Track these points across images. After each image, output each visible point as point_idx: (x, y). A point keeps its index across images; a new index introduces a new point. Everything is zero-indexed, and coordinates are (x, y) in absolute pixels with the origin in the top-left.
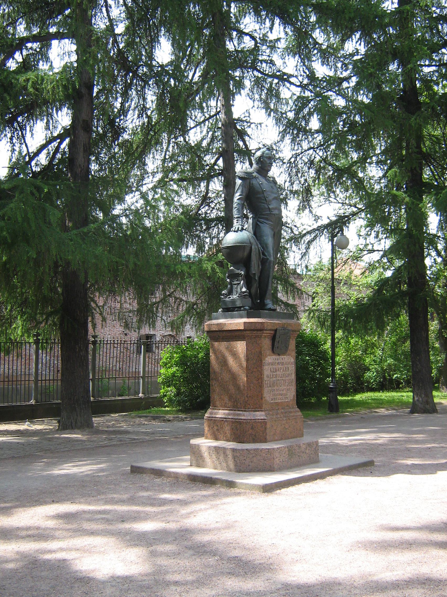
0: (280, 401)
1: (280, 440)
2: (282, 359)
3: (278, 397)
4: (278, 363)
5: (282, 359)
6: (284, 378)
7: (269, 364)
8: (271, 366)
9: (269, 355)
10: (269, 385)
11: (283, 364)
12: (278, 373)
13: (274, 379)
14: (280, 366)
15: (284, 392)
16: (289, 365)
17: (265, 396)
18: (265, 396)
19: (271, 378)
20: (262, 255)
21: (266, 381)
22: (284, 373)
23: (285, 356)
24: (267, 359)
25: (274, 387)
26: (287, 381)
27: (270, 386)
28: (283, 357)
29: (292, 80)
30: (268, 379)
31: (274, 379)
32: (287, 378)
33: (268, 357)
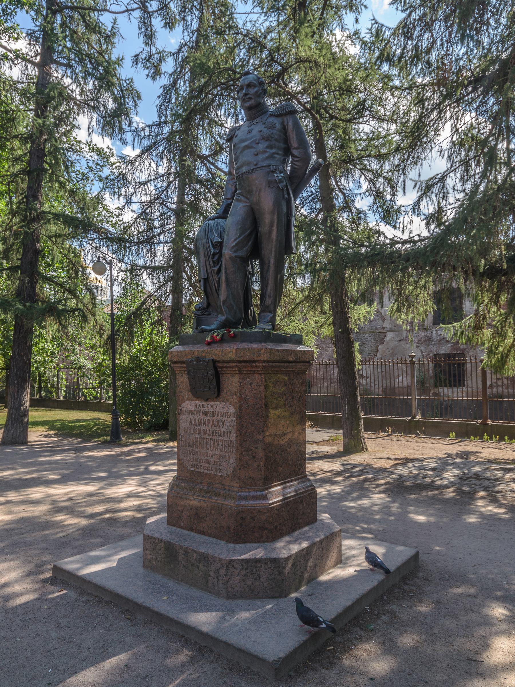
0: (206, 471)
2: (212, 407)
3: (203, 464)
4: (204, 413)
5: (212, 407)
6: (215, 438)
7: (188, 412)
8: (191, 416)
9: (188, 399)
11: (213, 414)
12: (203, 427)
13: (197, 436)
14: (208, 418)
16: (226, 418)
20: (212, 248)
23: (217, 403)
24: (184, 404)
25: (196, 447)
26: (221, 443)
27: (189, 446)
28: (212, 403)
32: (220, 438)
33: (187, 402)
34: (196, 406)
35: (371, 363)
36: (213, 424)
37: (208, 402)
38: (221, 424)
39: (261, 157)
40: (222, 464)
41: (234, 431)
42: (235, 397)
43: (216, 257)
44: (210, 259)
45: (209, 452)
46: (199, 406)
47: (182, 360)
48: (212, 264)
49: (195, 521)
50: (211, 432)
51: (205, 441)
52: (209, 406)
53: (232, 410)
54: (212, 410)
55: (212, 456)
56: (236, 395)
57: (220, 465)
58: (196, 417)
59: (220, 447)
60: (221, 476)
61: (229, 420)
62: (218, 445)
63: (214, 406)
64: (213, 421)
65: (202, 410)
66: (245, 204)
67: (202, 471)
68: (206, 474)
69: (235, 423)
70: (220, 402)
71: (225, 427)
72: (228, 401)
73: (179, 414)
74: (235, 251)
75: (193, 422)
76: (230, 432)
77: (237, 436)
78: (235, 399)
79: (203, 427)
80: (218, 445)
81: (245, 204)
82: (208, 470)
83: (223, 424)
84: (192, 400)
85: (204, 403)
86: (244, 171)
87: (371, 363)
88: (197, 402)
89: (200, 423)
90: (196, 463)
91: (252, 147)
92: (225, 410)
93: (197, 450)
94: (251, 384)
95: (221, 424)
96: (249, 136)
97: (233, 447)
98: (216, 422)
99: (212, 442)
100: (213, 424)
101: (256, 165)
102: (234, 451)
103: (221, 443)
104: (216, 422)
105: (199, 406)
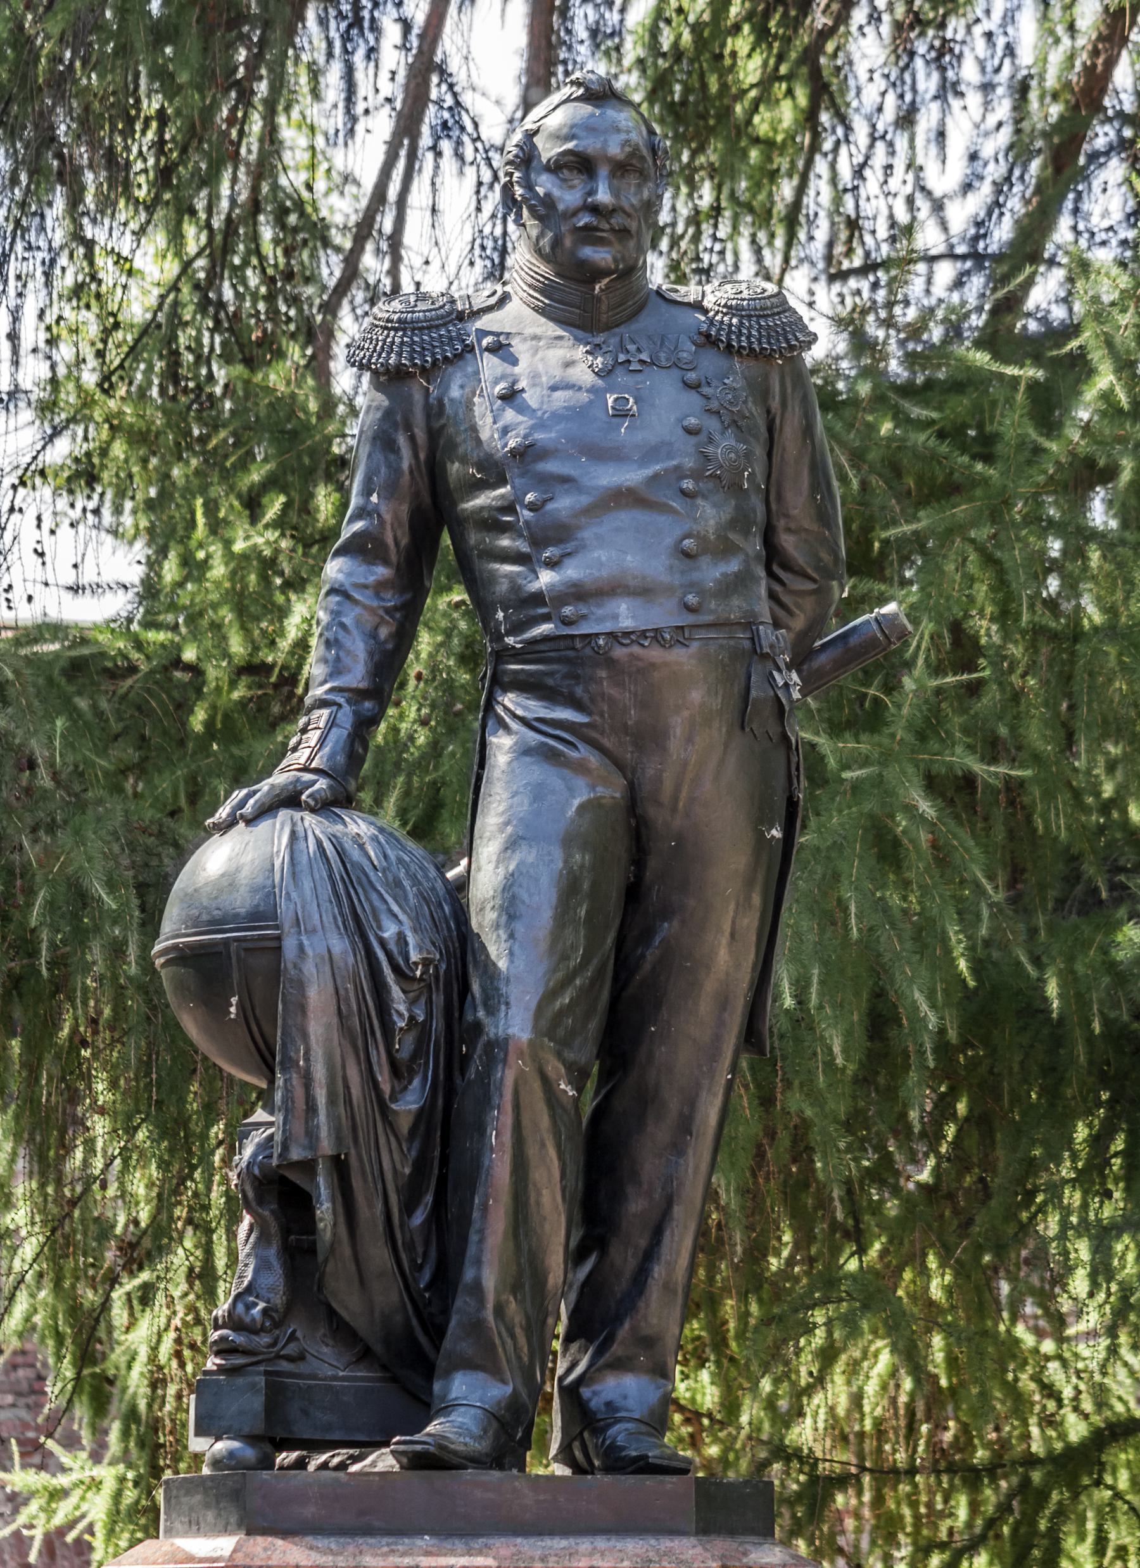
20: (396, 992)
39: (713, 572)
48: (384, 1079)
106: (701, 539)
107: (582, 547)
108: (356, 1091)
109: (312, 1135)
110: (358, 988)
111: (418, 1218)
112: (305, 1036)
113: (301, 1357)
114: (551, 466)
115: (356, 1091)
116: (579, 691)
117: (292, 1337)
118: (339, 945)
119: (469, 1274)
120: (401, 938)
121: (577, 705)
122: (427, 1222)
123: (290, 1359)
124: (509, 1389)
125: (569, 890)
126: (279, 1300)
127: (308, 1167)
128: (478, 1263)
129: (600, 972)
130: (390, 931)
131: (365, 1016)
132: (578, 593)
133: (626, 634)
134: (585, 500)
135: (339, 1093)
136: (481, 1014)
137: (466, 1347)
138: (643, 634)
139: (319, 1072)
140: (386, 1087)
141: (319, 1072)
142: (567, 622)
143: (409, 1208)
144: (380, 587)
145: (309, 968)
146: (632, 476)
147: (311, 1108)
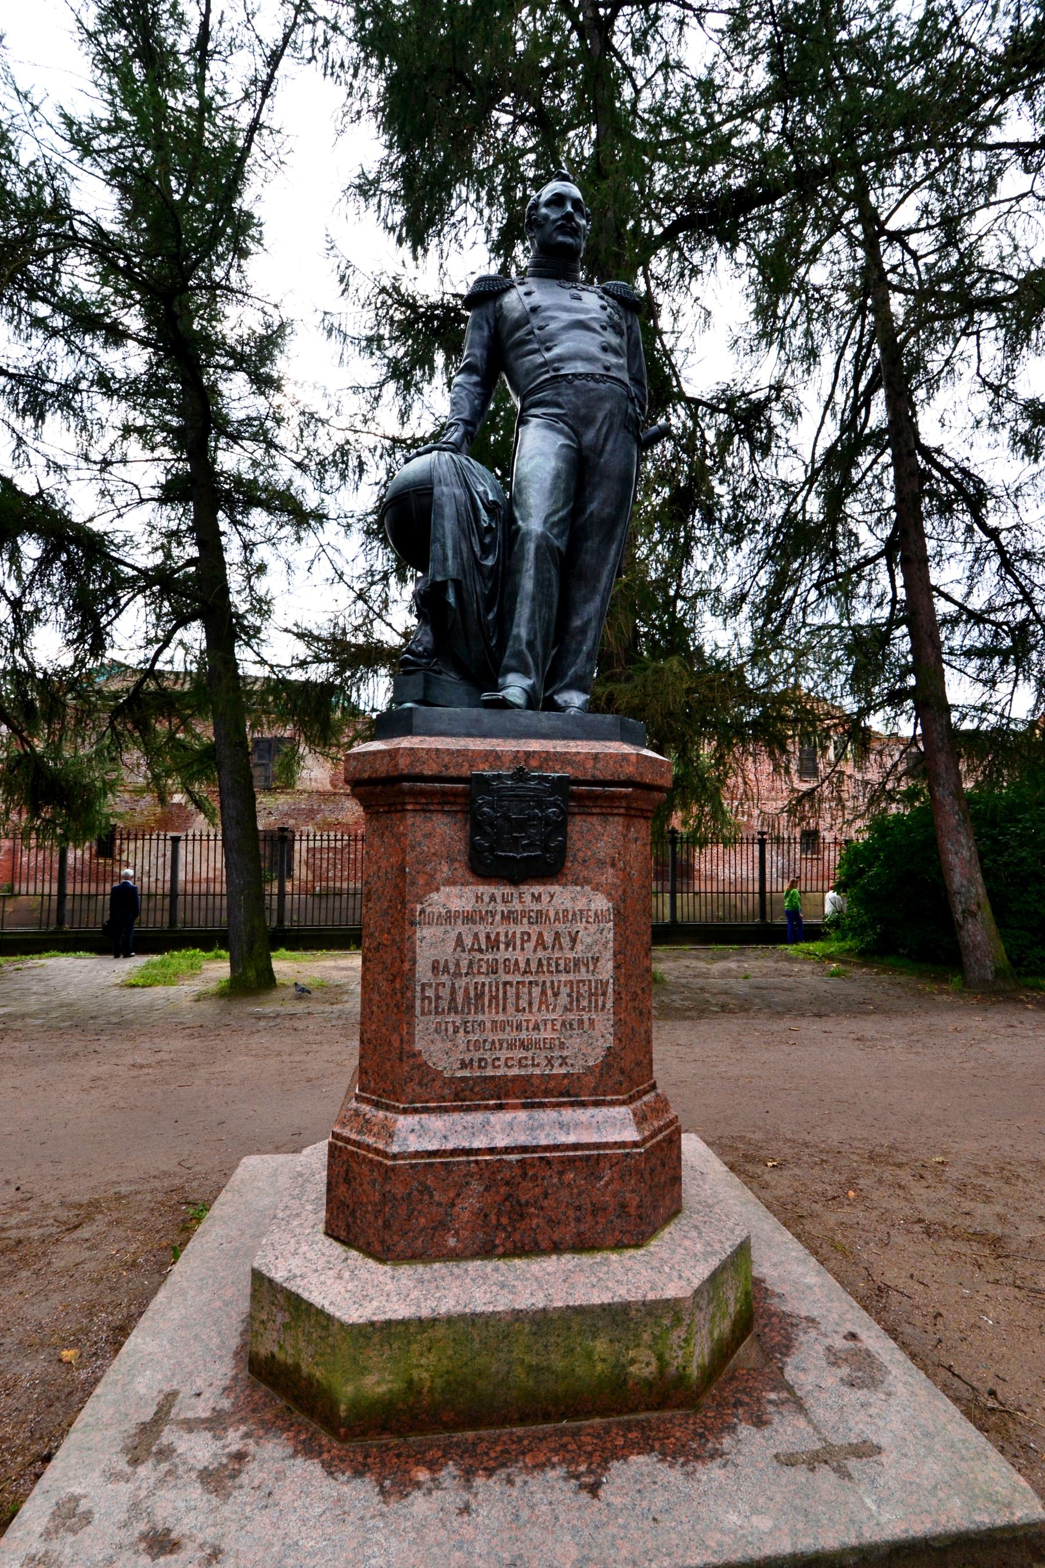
0: (515, 1071)
1: (474, 1256)
2: (537, 898)
3: (503, 1054)
4: (506, 917)
6: (547, 978)
7: (449, 917)
8: (461, 928)
9: (451, 882)
10: (444, 1004)
11: (540, 917)
12: (502, 954)
13: (481, 979)
15: (547, 1034)
16: (580, 926)
17: (418, 1046)
18: (418, 1046)
19: (457, 974)
20: (483, 512)
21: (423, 986)
22: (540, 954)
23: (556, 888)
25: (480, 1009)
26: (565, 990)
27: (453, 1008)
28: (537, 889)
29: (1038, 179)
30: (444, 978)
31: (481, 979)
32: (563, 977)
33: (445, 889)
34: (479, 898)
35: (325, 837)
36: (541, 942)
37: (524, 888)
38: (565, 941)
39: (612, 359)
40: (568, 1043)
41: (609, 954)
42: (611, 871)
43: (487, 540)
44: (475, 541)
45: (527, 1016)
46: (493, 898)
47: (453, 772)
49: (504, 1221)
50: (534, 967)
51: (511, 991)
52: (528, 898)
53: (601, 903)
54: (536, 907)
55: (536, 1028)
56: (613, 865)
57: (562, 1046)
58: (482, 929)
59: (563, 999)
60: (565, 1076)
61: (593, 928)
62: (556, 995)
63: (545, 898)
64: (540, 934)
65: (500, 907)
66: (568, 442)
67: (499, 1073)
68: (516, 1078)
69: (611, 936)
70: (565, 885)
71: (579, 947)
72: (587, 881)
73: (413, 923)
74: (557, 537)
75: (468, 941)
76: (596, 960)
77: (617, 967)
78: (609, 875)
79: (502, 954)
80: (556, 995)
81: (568, 442)
82: (521, 1066)
83: (574, 940)
84: (468, 884)
85: (507, 890)
86: (581, 370)
87: (325, 837)
88: (481, 889)
89: (493, 944)
90: (477, 1055)
91: (593, 330)
92: (581, 904)
93: (480, 1017)
94: (636, 840)
95: (565, 941)
96: (576, 304)
97: (604, 994)
98: (548, 938)
99: (536, 991)
100: (541, 942)
101: (607, 369)
102: (609, 1004)
103: (565, 990)
104: (548, 938)
105: (493, 898)
106: (609, 344)
107: (562, 342)
108: (465, 555)
109: (445, 569)
110: (467, 510)
111: (491, 616)
112: (443, 527)
113: (440, 673)
114: (549, 313)
115: (465, 555)
116: (560, 400)
117: (436, 664)
118: (458, 491)
119: (515, 631)
120: (485, 492)
121: (558, 405)
122: (496, 617)
123: (434, 671)
124: (531, 682)
125: (557, 476)
126: (430, 646)
127: (443, 585)
128: (519, 626)
129: (568, 514)
130: (481, 489)
131: (469, 523)
132: (561, 359)
133: (581, 374)
134: (562, 324)
135: (458, 552)
136: (520, 523)
137: (513, 663)
138: (587, 375)
139: (449, 543)
140: (478, 554)
141: (449, 543)
142: (556, 370)
143: (488, 610)
144: (475, 384)
145: (444, 499)
146: (582, 317)
147: (445, 558)
